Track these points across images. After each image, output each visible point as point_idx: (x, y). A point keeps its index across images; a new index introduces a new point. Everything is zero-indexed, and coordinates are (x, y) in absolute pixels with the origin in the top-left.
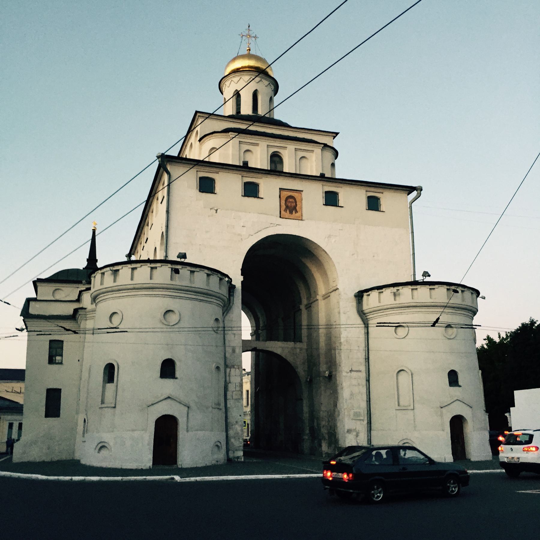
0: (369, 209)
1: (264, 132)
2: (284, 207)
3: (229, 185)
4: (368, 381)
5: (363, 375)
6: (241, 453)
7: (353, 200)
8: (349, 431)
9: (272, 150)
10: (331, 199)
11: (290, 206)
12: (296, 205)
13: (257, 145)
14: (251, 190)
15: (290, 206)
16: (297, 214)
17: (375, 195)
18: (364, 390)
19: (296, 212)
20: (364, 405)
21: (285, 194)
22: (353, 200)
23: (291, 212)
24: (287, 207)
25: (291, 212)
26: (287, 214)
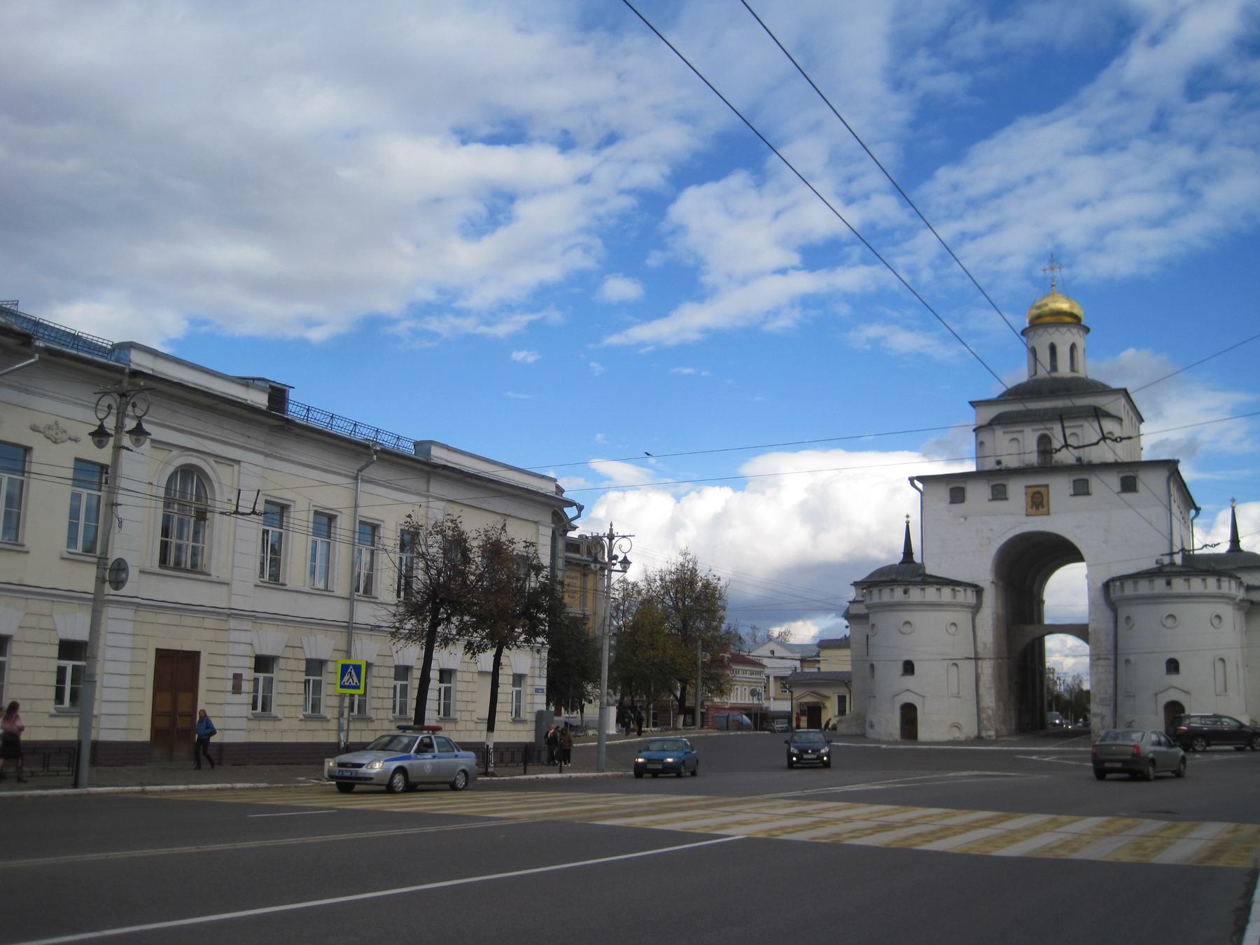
3: (978, 494)
4: (1116, 667)
5: (1112, 662)
6: (992, 733)
7: (1104, 486)
8: (1096, 715)
9: (1038, 434)
11: (1038, 502)
15: (1038, 502)
17: (1129, 475)
18: (1111, 677)
20: (1111, 690)
21: (1031, 491)
22: (1104, 486)
23: (1037, 508)
25: (1037, 508)
26: (1034, 511)
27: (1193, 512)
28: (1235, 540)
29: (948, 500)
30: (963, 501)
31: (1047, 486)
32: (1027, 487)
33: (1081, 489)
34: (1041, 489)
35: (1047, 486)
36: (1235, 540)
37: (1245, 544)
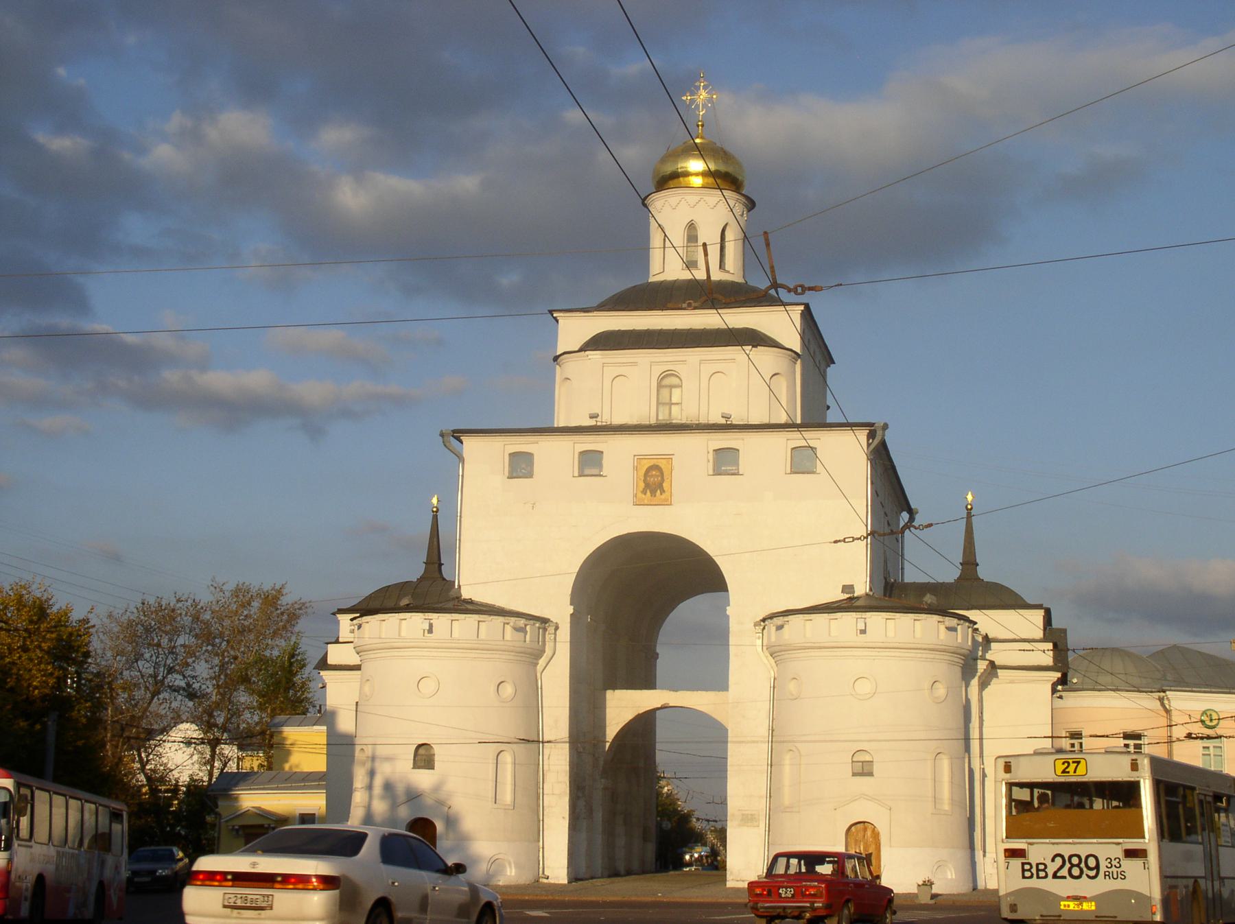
0: (792, 472)
1: (661, 333)
2: (642, 485)
9: (657, 371)
10: (725, 462)
11: (654, 482)
12: (663, 480)
13: (635, 364)
14: (590, 462)
15: (654, 482)
16: (663, 497)
19: (663, 491)
21: (647, 464)
23: (653, 493)
24: (647, 485)
25: (653, 493)
27: (905, 516)
28: (969, 563)
29: (507, 474)
30: (531, 476)
31: (669, 458)
32: (640, 458)
33: (725, 462)
34: (662, 464)
35: (669, 458)
36: (969, 563)
37: (985, 573)
